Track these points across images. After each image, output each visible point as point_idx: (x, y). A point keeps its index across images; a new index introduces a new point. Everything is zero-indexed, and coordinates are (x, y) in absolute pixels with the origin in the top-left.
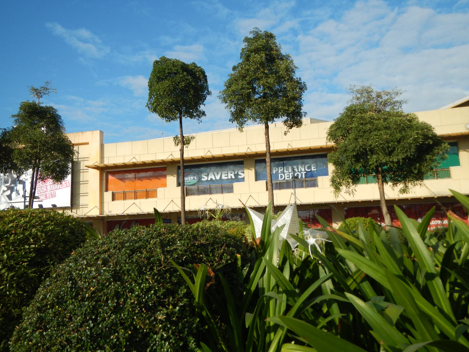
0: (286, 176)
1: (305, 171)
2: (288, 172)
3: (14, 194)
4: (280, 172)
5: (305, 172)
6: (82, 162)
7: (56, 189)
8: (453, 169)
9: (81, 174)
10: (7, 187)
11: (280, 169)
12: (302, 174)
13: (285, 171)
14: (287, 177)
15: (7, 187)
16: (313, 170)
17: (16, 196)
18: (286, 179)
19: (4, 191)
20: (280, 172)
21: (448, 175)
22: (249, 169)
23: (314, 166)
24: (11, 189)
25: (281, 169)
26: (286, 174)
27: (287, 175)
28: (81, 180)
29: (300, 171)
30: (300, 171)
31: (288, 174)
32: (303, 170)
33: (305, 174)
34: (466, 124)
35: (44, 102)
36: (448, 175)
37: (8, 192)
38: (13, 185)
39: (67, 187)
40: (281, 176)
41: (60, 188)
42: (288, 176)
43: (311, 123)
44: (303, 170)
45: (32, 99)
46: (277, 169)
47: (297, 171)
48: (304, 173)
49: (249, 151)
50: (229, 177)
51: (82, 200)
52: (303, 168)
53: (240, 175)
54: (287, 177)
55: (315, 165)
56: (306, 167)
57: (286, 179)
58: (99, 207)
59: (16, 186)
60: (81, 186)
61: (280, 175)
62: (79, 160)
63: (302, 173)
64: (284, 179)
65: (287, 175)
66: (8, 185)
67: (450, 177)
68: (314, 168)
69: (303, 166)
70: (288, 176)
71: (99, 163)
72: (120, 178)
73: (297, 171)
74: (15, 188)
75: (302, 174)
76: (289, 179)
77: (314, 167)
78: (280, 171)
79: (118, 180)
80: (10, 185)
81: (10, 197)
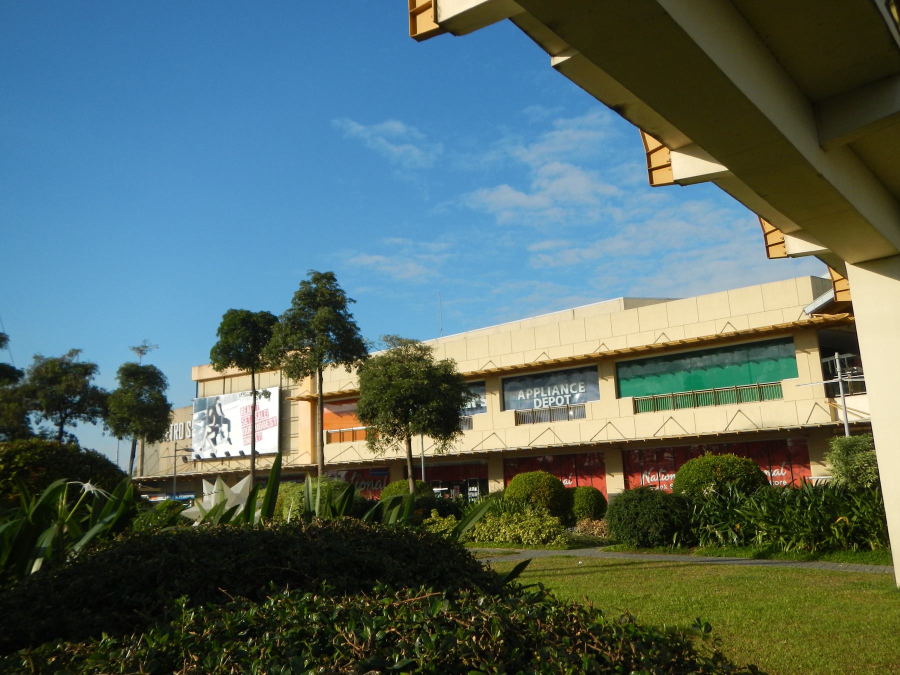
1: (570, 393)
2: (546, 395)
3: (219, 436)
4: (535, 396)
5: (570, 396)
6: (292, 391)
7: (263, 429)
8: (787, 385)
9: (292, 407)
10: (211, 427)
11: (535, 391)
12: (565, 399)
13: (543, 395)
14: (546, 404)
15: (211, 427)
17: (221, 439)
18: (544, 406)
19: (209, 434)
20: (535, 396)
21: (777, 394)
22: (492, 393)
23: (582, 385)
24: (215, 430)
25: (537, 391)
26: (544, 399)
27: (546, 400)
28: (292, 416)
29: (562, 393)
30: (562, 393)
31: (547, 398)
32: (567, 392)
33: (570, 398)
34: (804, 306)
35: (145, 361)
36: (777, 394)
37: (213, 435)
38: (217, 425)
39: (274, 426)
40: (538, 403)
41: (266, 428)
42: (547, 402)
43: (626, 308)
44: (567, 392)
45: (134, 359)
46: (532, 391)
47: (558, 393)
48: (568, 397)
49: (491, 367)
51: (294, 444)
52: (567, 389)
53: (484, 403)
54: (546, 404)
55: (583, 383)
56: (571, 386)
57: (544, 406)
58: (310, 452)
59: (221, 426)
60: (292, 423)
61: (535, 400)
62: (290, 388)
63: (565, 396)
64: (542, 406)
65: (546, 400)
66: (212, 425)
67: (782, 397)
68: (582, 389)
70: (547, 402)
71: (310, 390)
72: (337, 411)
73: (558, 393)
74: (220, 429)
75: (565, 399)
76: (547, 406)
77: (582, 387)
78: (536, 394)
79: (334, 415)
80: (215, 425)
81: (214, 441)
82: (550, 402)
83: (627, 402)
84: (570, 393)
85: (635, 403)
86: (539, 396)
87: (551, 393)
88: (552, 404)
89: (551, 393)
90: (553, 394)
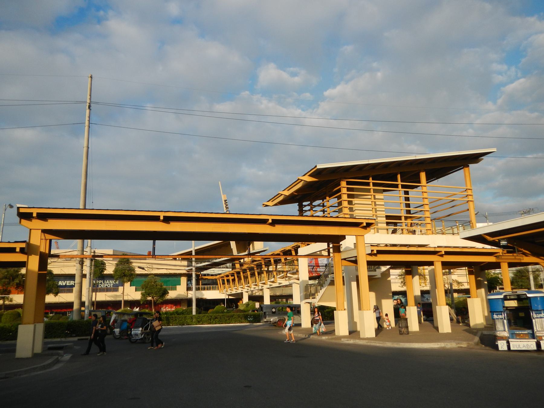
0: (103, 285)
1: (113, 283)
4: (99, 283)
8: (178, 287)
12: (111, 285)
13: (102, 283)
16: (117, 283)
21: (176, 289)
26: (103, 284)
29: (110, 283)
30: (110, 283)
33: (113, 285)
36: (176, 289)
40: (100, 286)
44: (112, 283)
47: (109, 283)
48: (112, 285)
50: (71, 285)
57: (103, 287)
69: (112, 281)
75: (111, 285)
82: (105, 286)
83: (134, 288)
84: (113, 283)
85: (136, 288)
86: (101, 283)
87: (106, 282)
88: (106, 286)
89: (106, 282)
90: (107, 283)
